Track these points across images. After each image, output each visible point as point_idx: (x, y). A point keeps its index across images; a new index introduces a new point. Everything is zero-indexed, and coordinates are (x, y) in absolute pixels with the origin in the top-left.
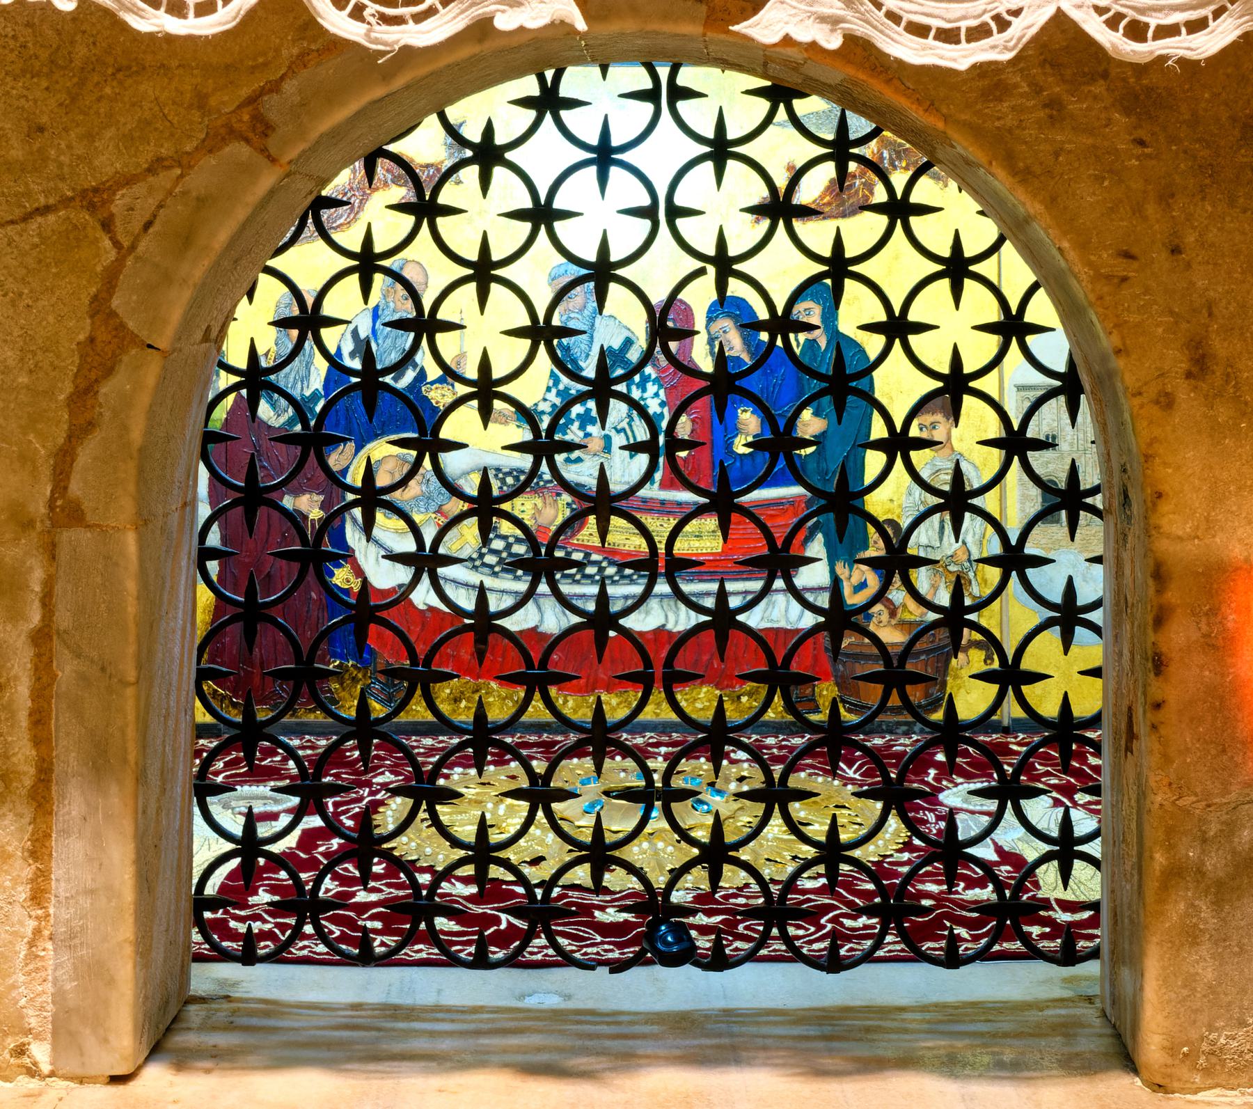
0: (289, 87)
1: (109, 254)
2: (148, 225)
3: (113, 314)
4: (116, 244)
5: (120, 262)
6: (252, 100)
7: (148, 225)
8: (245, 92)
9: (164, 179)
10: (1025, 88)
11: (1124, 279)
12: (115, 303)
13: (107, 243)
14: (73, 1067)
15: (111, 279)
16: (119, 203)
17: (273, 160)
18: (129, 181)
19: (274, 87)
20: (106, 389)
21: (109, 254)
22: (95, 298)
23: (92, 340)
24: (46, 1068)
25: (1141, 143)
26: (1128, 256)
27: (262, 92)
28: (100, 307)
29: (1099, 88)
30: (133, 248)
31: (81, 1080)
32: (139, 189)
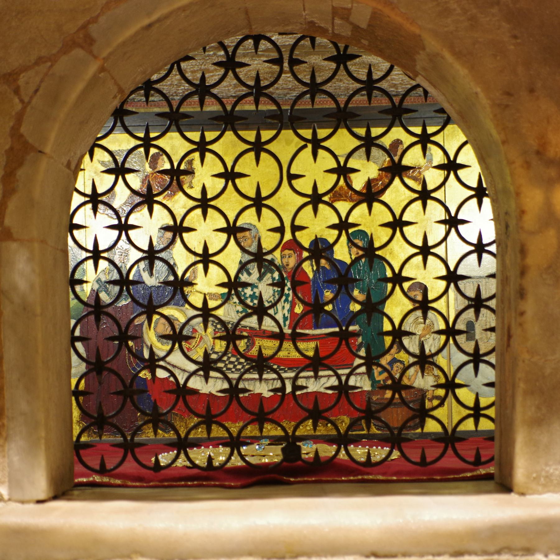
0: (102, 19)
1: (19, 107)
2: (36, 91)
3: (22, 136)
4: (22, 101)
5: (24, 109)
6: (84, 27)
7: (36, 91)
8: (80, 23)
9: (43, 68)
10: (459, 11)
11: (507, 106)
12: (23, 130)
13: (17, 100)
14: (18, 495)
15: (20, 118)
16: (21, 81)
17: (95, 57)
18: (25, 69)
19: (94, 20)
20: (21, 173)
21: (19, 107)
22: (13, 128)
23: (11, 149)
24: (6, 497)
25: (515, 37)
26: (509, 94)
27: (89, 22)
28: (15, 133)
29: (495, 10)
30: (29, 102)
31: (23, 502)
32: (31, 73)
